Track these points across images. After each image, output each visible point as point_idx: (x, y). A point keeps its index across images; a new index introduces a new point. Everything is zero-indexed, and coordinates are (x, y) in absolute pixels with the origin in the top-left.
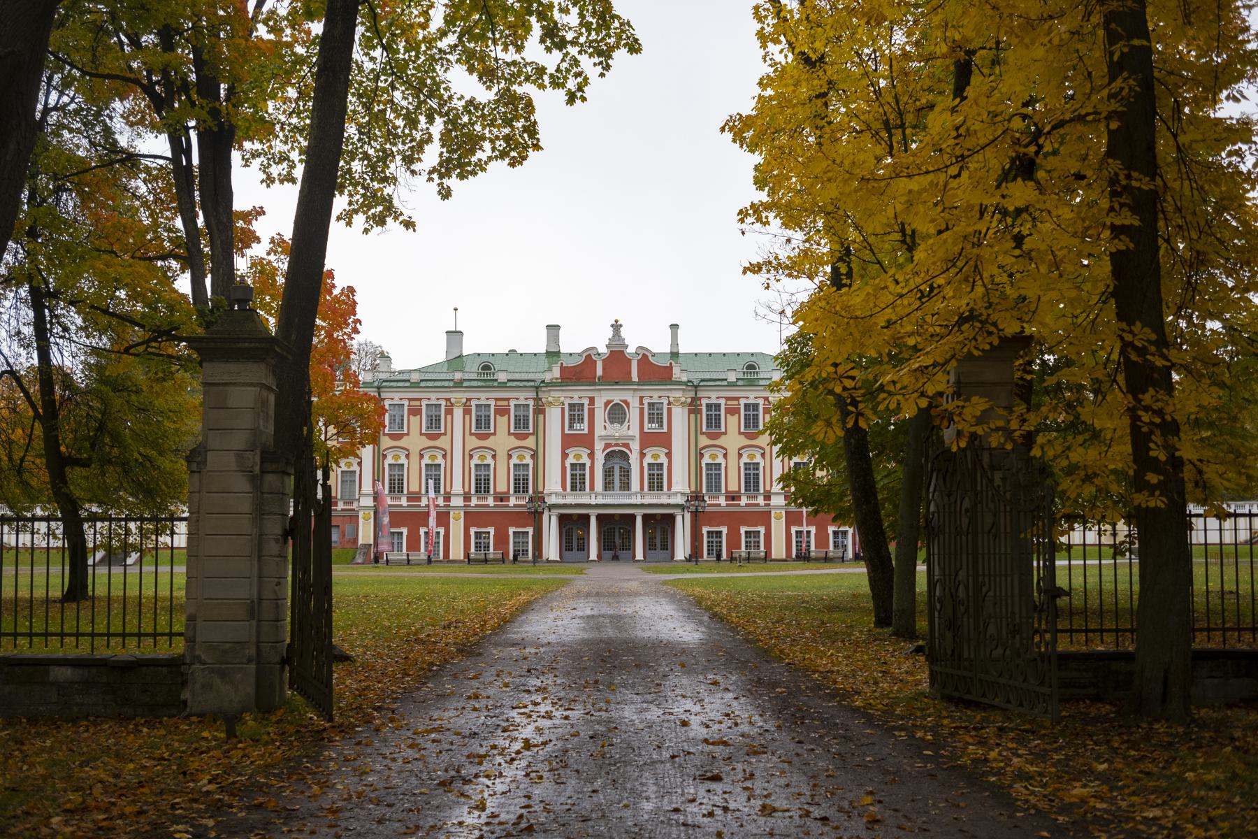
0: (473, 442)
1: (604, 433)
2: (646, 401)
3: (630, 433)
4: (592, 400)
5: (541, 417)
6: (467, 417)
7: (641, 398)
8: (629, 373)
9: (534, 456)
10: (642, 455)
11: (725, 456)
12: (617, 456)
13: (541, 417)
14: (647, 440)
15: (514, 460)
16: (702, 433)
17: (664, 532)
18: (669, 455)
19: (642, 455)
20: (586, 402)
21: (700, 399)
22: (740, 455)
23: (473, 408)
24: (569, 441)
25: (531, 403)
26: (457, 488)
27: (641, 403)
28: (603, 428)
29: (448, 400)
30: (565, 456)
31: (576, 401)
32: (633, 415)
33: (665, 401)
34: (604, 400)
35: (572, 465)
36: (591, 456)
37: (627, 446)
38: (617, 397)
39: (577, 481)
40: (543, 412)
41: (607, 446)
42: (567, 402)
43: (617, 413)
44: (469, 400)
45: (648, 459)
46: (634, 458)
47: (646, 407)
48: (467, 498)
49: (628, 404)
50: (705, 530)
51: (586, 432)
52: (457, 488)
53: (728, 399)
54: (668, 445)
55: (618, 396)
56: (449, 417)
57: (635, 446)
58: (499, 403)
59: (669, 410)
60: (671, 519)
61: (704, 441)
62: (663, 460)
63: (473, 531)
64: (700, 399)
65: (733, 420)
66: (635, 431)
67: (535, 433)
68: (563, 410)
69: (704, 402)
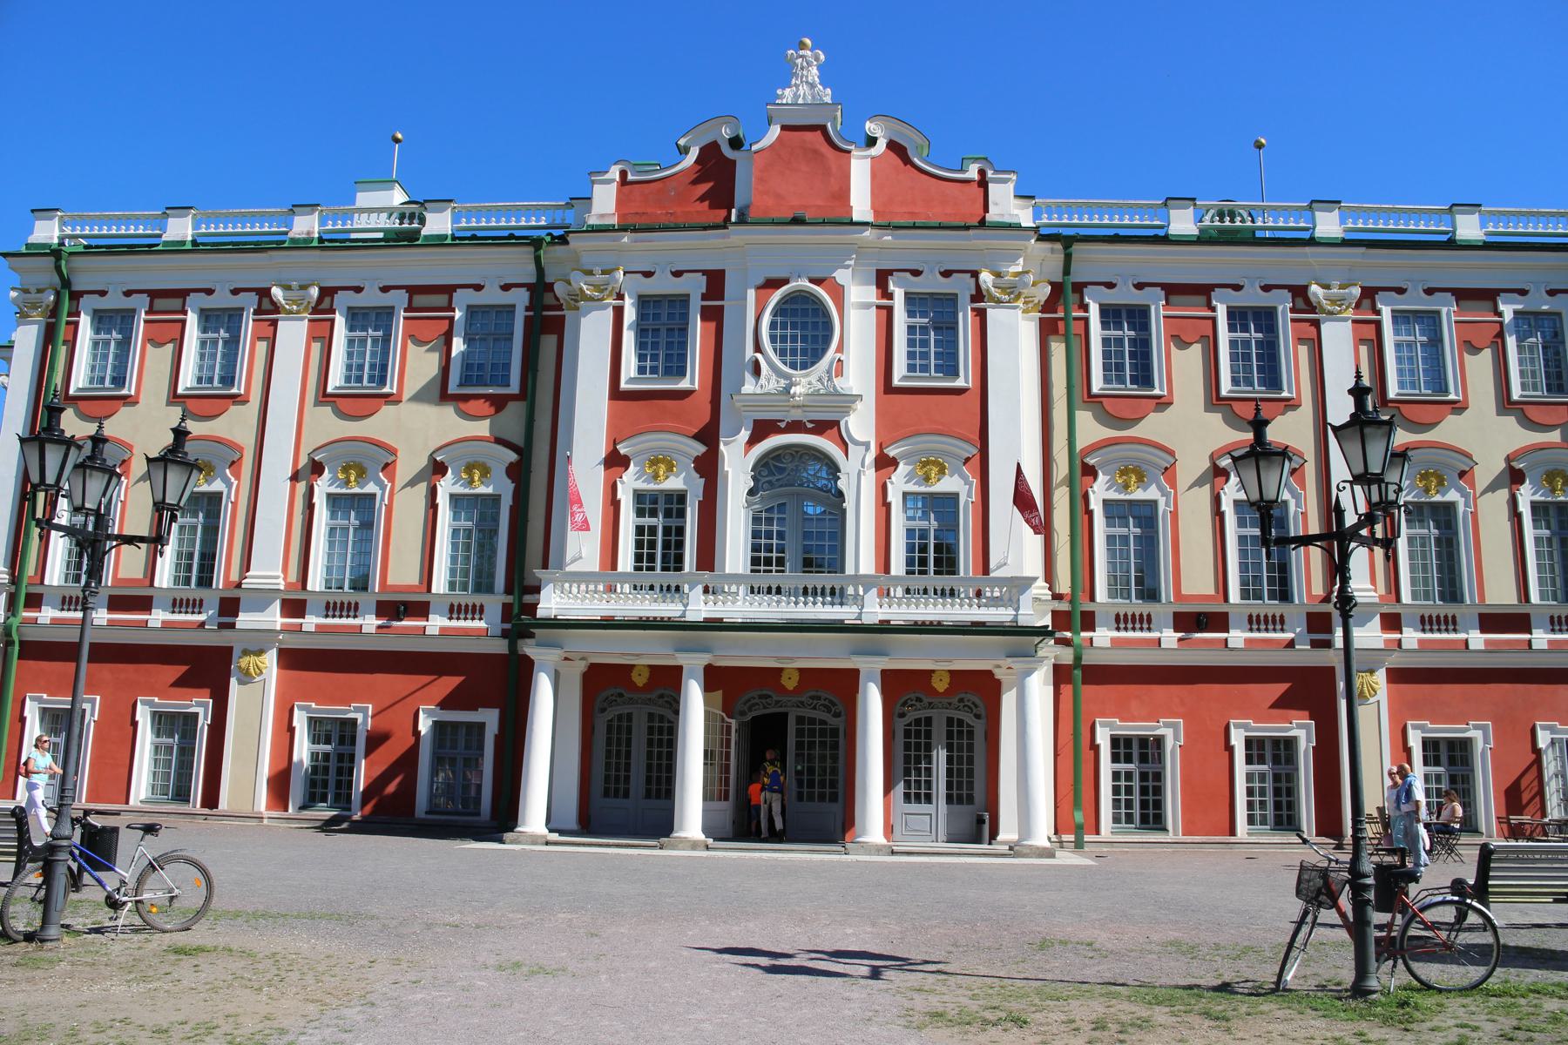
0: (327, 426)
4: (716, 282)
5: (549, 341)
8: (843, 194)
10: (885, 463)
13: (549, 341)
17: (959, 739)
20: (695, 286)
25: (520, 298)
26: (269, 570)
30: (616, 461)
31: (663, 285)
36: (708, 467)
40: (557, 326)
46: (858, 482)
52: (269, 570)
57: (861, 424)
60: (982, 692)
67: (527, 393)
68: (619, 312)
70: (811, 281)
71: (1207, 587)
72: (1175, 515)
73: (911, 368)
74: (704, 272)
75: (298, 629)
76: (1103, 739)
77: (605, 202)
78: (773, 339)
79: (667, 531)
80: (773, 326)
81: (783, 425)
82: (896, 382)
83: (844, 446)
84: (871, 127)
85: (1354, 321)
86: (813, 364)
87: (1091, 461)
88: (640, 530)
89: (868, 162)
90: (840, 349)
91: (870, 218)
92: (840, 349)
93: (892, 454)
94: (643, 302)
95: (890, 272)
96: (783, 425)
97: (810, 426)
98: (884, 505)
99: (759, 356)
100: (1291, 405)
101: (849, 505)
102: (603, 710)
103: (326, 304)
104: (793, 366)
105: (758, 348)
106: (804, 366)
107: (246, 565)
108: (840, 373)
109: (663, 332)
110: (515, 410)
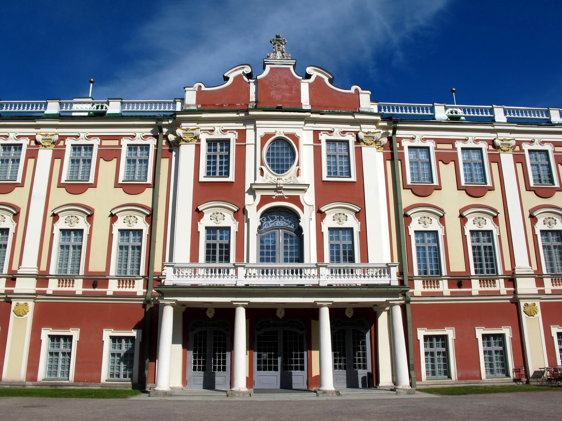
0: (61, 197)
1: (260, 180)
2: (323, 138)
3: (300, 180)
4: (242, 134)
6: (58, 162)
7: (316, 133)
9: (151, 218)
10: (321, 215)
11: (442, 219)
12: (281, 215)
14: (327, 192)
15: (120, 224)
16: (406, 187)
18: (361, 215)
19: (321, 215)
20: (233, 137)
21: (399, 140)
22: (463, 219)
23: (68, 151)
24: (203, 192)
27: (317, 140)
28: (256, 171)
29: (32, 138)
30: (198, 214)
32: (305, 155)
33: (351, 139)
34: (261, 132)
35: (208, 229)
37: (296, 200)
38: (280, 129)
39: (218, 249)
41: (265, 200)
42: (204, 137)
43: (282, 153)
44: (63, 138)
45: (328, 222)
47: (324, 145)
48: (42, 278)
49: (296, 139)
50: (421, 333)
51: (231, 178)
53: (438, 141)
54: (360, 201)
55: (280, 129)
56: (31, 162)
57: (309, 198)
58: (105, 143)
59: (359, 152)
61: (408, 198)
62: (352, 222)
63: (45, 333)
64: (399, 140)
65: (448, 170)
66: (307, 176)
68: (198, 147)
69: (406, 144)
70: (285, 135)
71: (463, 269)
72: (445, 237)
73: (329, 173)
74: (237, 130)
75: (44, 293)
76: (421, 338)
77: (191, 98)
78: (268, 160)
79: (221, 245)
80: (268, 154)
81: (274, 197)
82: (325, 178)
83: (302, 207)
84: (309, 70)
85: (513, 154)
86: (286, 171)
87: (409, 213)
88: (208, 246)
89: (307, 85)
90: (298, 165)
91: (309, 108)
92: (298, 165)
93: (323, 211)
94: (210, 142)
95: (320, 131)
96: (274, 197)
97: (286, 198)
98: (320, 235)
99: (263, 167)
100: (492, 189)
101: (305, 233)
102: (192, 330)
103: (61, 143)
104: (278, 172)
105: (262, 164)
106: (283, 172)
107: (20, 264)
108: (298, 175)
109: (218, 158)
110: (149, 192)
